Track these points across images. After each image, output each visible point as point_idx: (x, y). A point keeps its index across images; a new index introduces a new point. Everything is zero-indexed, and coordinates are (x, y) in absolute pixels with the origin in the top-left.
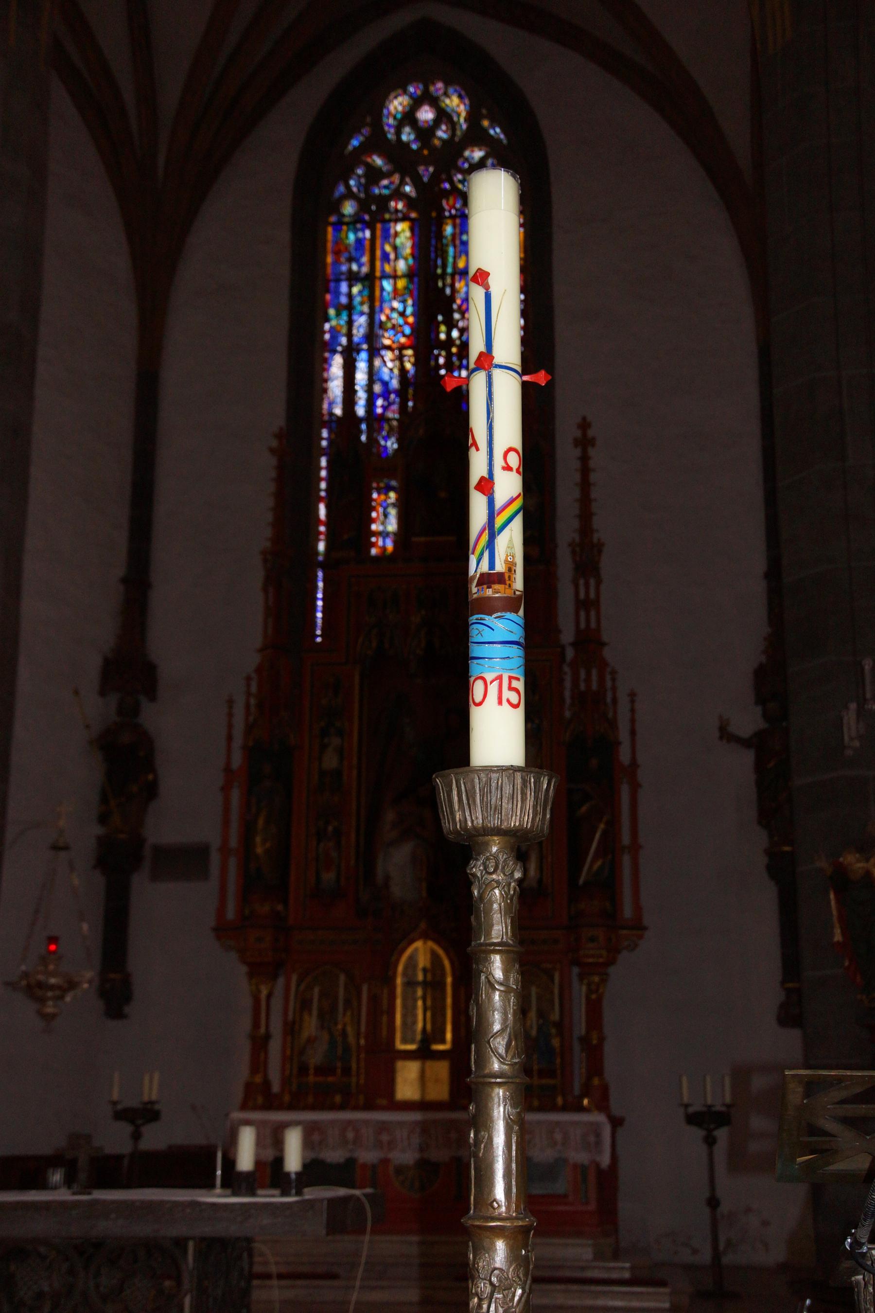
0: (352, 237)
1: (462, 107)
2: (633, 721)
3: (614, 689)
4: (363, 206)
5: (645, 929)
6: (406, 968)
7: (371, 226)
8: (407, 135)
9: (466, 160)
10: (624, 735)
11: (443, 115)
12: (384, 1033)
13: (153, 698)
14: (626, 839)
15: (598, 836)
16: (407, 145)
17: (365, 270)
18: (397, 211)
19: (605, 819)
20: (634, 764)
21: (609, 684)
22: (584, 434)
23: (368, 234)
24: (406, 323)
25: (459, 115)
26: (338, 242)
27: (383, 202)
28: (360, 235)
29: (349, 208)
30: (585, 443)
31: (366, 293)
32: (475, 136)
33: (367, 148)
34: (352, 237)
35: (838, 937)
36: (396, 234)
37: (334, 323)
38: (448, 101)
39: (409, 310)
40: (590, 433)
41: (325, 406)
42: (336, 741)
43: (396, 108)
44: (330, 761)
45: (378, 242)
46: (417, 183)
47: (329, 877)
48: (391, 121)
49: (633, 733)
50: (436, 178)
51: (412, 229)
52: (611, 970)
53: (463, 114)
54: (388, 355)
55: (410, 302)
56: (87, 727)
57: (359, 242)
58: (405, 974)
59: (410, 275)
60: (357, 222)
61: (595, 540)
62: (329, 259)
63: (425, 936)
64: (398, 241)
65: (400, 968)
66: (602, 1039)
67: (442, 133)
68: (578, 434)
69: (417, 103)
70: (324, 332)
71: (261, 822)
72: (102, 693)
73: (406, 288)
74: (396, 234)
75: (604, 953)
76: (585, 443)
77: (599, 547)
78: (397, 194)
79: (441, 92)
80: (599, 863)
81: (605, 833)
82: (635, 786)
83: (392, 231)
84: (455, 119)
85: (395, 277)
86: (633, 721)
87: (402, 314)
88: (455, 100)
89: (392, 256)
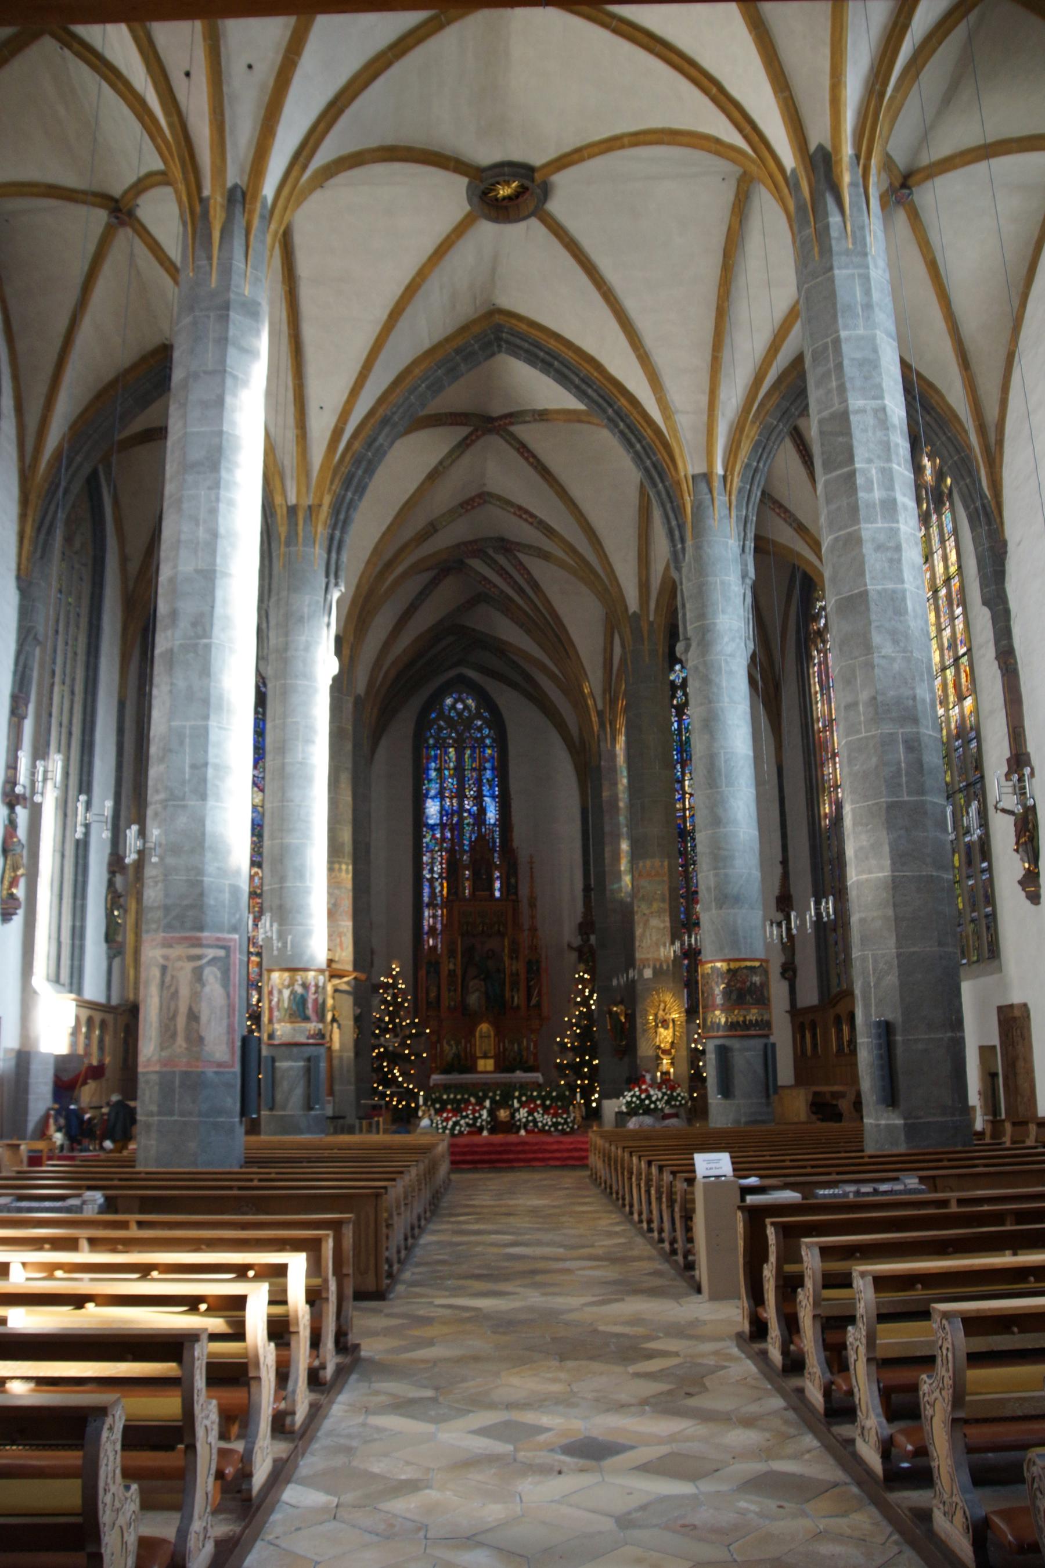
0: (433, 753)
4: (437, 741)
7: (438, 748)
8: (453, 714)
11: (466, 707)
26: (428, 754)
27: (444, 739)
29: (431, 741)
32: (479, 716)
33: (438, 718)
46: (457, 733)
50: (463, 730)
54: (448, 800)
57: (436, 756)
59: (455, 769)
60: (435, 747)
67: (466, 714)
69: (456, 701)
78: (450, 737)
85: (449, 769)
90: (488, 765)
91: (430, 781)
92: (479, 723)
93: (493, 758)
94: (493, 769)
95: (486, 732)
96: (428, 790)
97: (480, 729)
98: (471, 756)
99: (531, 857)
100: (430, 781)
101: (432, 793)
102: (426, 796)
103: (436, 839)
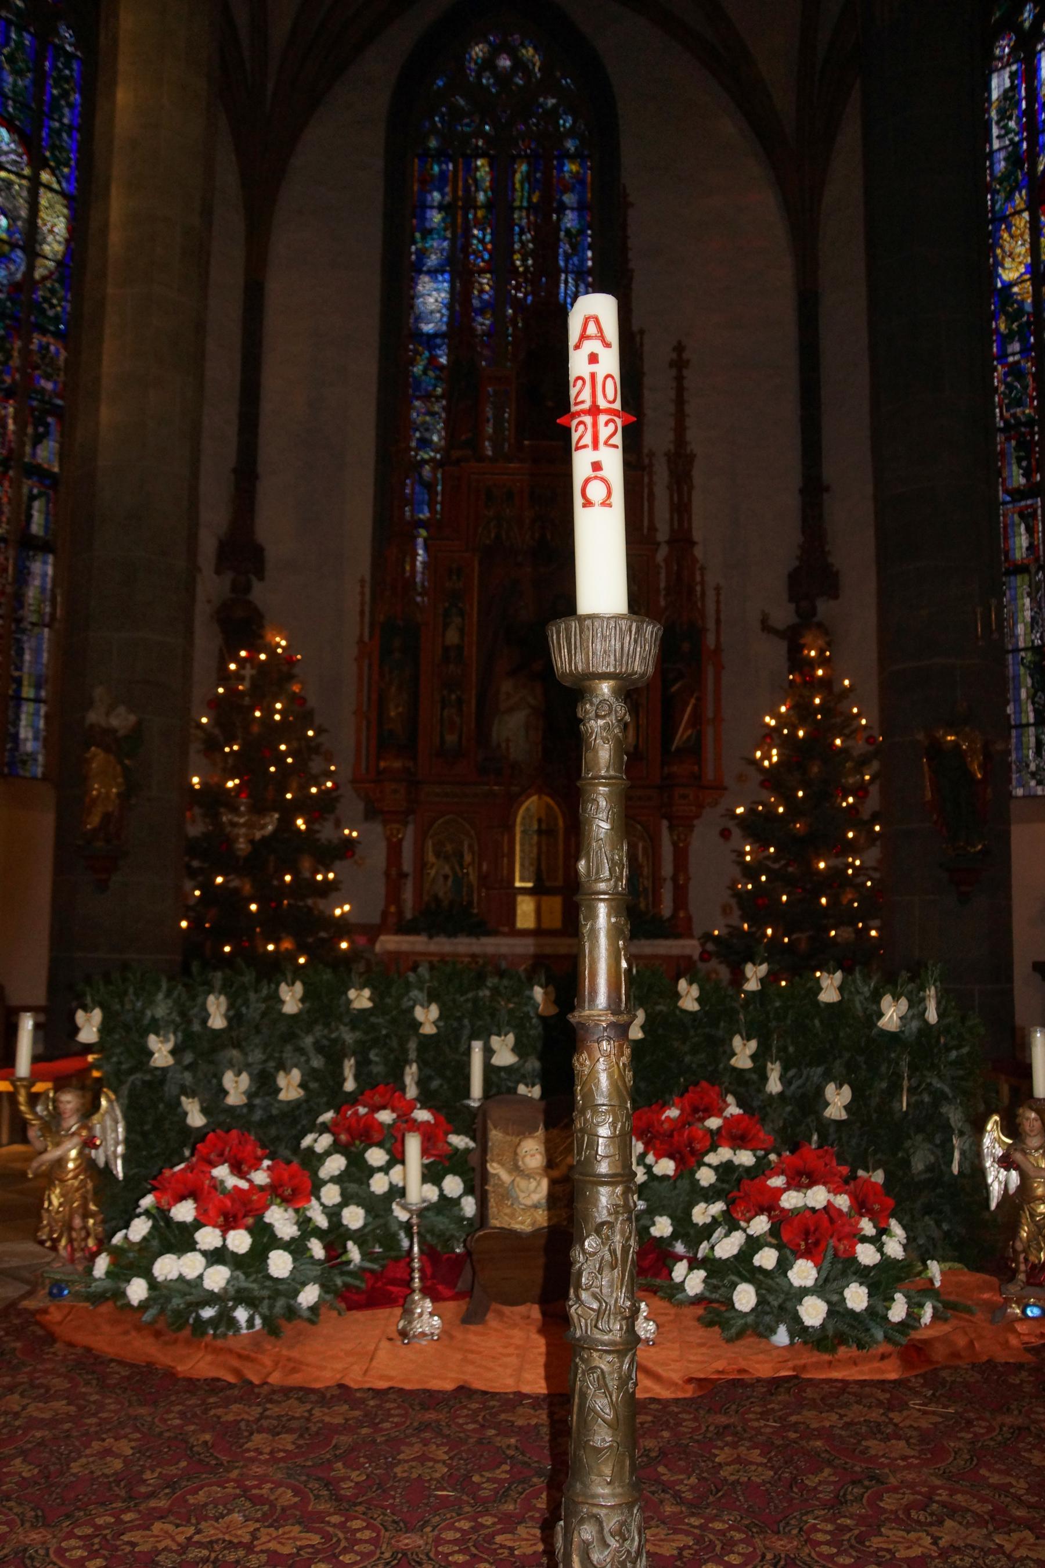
1: (537, 57)
2: (718, 611)
3: (703, 583)
5: (726, 789)
6: (524, 818)
9: (541, 106)
10: (711, 624)
11: (519, 64)
12: (505, 872)
13: (261, 578)
14: (710, 714)
15: (689, 709)
16: (487, 88)
17: (448, 199)
18: (477, 146)
19: (695, 695)
20: (718, 649)
21: (698, 578)
22: (680, 355)
23: (451, 166)
24: (485, 249)
25: (534, 65)
28: (444, 167)
30: (679, 364)
31: (449, 220)
34: (436, 168)
35: (929, 795)
36: (477, 168)
37: (420, 245)
38: (524, 51)
39: (488, 238)
40: (686, 356)
41: (412, 321)
42: (457, 620)
43: (477, 54)
44: (452, 637)
45: (461, 174)
47: (451, 738)
48: (473, 66)
49: (718, 621)
51: (491, 165)
52: (695, 822)
53: (538, 64)
55: (489, 231)
56: (209, 602)
57: (443, 173)
58: (523, 824)
60: (441, 155)
61: (688, 451)
62: (416, 188)
63: (540, 792)
64: (478, 174)
65: (519, 820)
66: (688, 879)
68: (674, 356)
69: (495, 51)
70: (411, 254)
71: (393, 689)
72: (218, 572)
73: (485, 217)
74: (477, 168)
75: (694, 808)
76: (679, 364)
77: (691, 458)
79: (518, 43)
80: (689, 732)
81: (695, 707)
82: (719, 668)
83: (473, 165)
84: (531, 67)
86: (718, 611)
87: (482, 241)
88: (531, 51)
89: (473, 189)
90: (569, 199)
91: (427, 233)
92: (551, 102)
93: (582, 182)
94: (581, 208)
95: (566, 122)
96: (422, 254)
97: (553, 115)
98: (527, 177)
99: (679, 348)
100: (427, 233)
101: (433, 260)
102: (418, 269)
103: (441, 368)
